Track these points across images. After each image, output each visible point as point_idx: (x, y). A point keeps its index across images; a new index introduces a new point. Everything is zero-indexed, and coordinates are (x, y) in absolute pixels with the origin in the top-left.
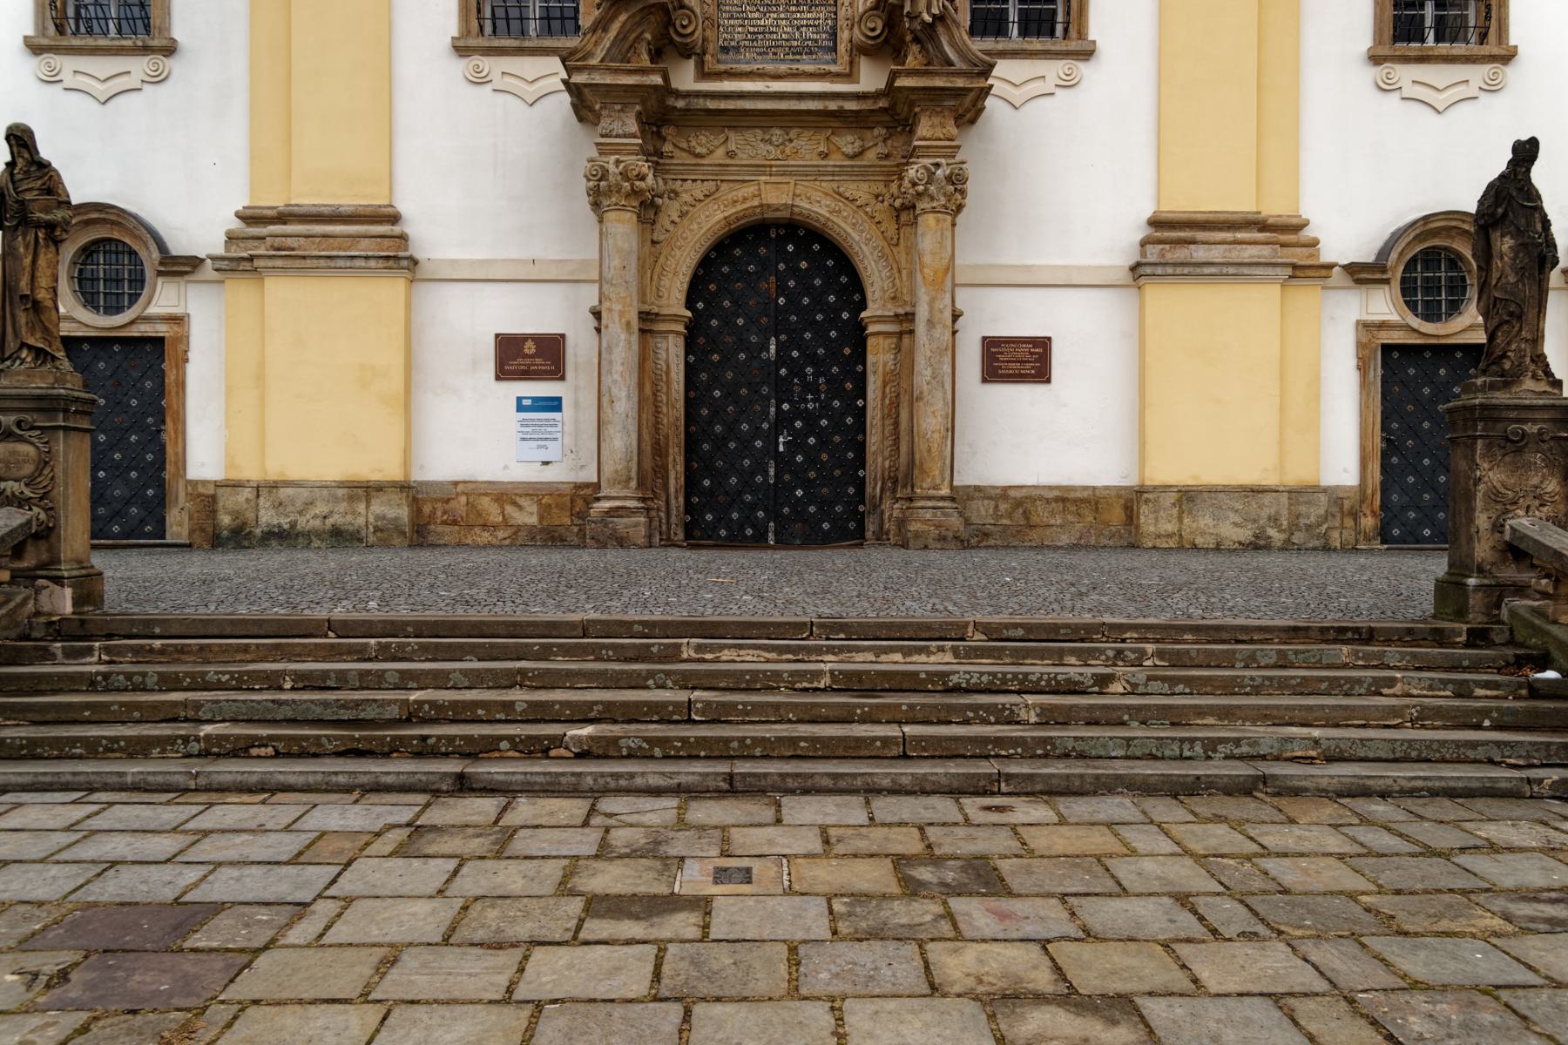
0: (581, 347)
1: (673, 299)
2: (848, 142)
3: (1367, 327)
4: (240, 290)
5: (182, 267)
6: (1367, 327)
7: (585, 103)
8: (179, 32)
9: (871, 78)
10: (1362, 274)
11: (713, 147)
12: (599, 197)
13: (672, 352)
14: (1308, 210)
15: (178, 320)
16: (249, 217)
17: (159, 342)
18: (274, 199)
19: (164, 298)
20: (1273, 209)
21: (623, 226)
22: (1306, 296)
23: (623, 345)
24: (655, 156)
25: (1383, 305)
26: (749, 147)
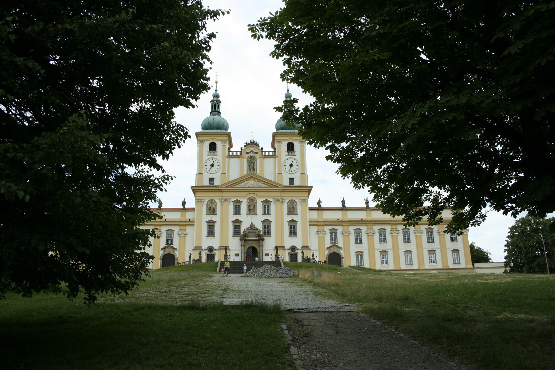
0: (240, 255)
1: (246, 252)
2: (256, 242)
3: (289, 253)
4: (220, 251)
5: (215, 250)
6: (289, 253)
7: (240, 240)
8: (215, 235)
9: (258, 238)
10: (288, 249)
11: (248, 242)
12: (241, 246)
13: (246, 255)
14: (285, 246)
15: (215, 253)
16: (220, 247)
17: (213, 255)
18: (221, 246)
19: (214, 252)
20: (282, 246)
21: (243, 247)
22: (284, 251)
23: (243, 254)
24: (245, 243)
25: (290, 251)
26: (250, 242)
